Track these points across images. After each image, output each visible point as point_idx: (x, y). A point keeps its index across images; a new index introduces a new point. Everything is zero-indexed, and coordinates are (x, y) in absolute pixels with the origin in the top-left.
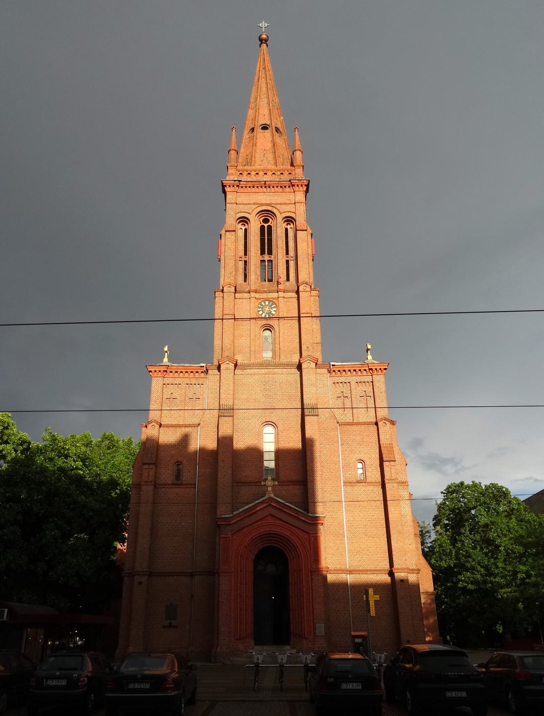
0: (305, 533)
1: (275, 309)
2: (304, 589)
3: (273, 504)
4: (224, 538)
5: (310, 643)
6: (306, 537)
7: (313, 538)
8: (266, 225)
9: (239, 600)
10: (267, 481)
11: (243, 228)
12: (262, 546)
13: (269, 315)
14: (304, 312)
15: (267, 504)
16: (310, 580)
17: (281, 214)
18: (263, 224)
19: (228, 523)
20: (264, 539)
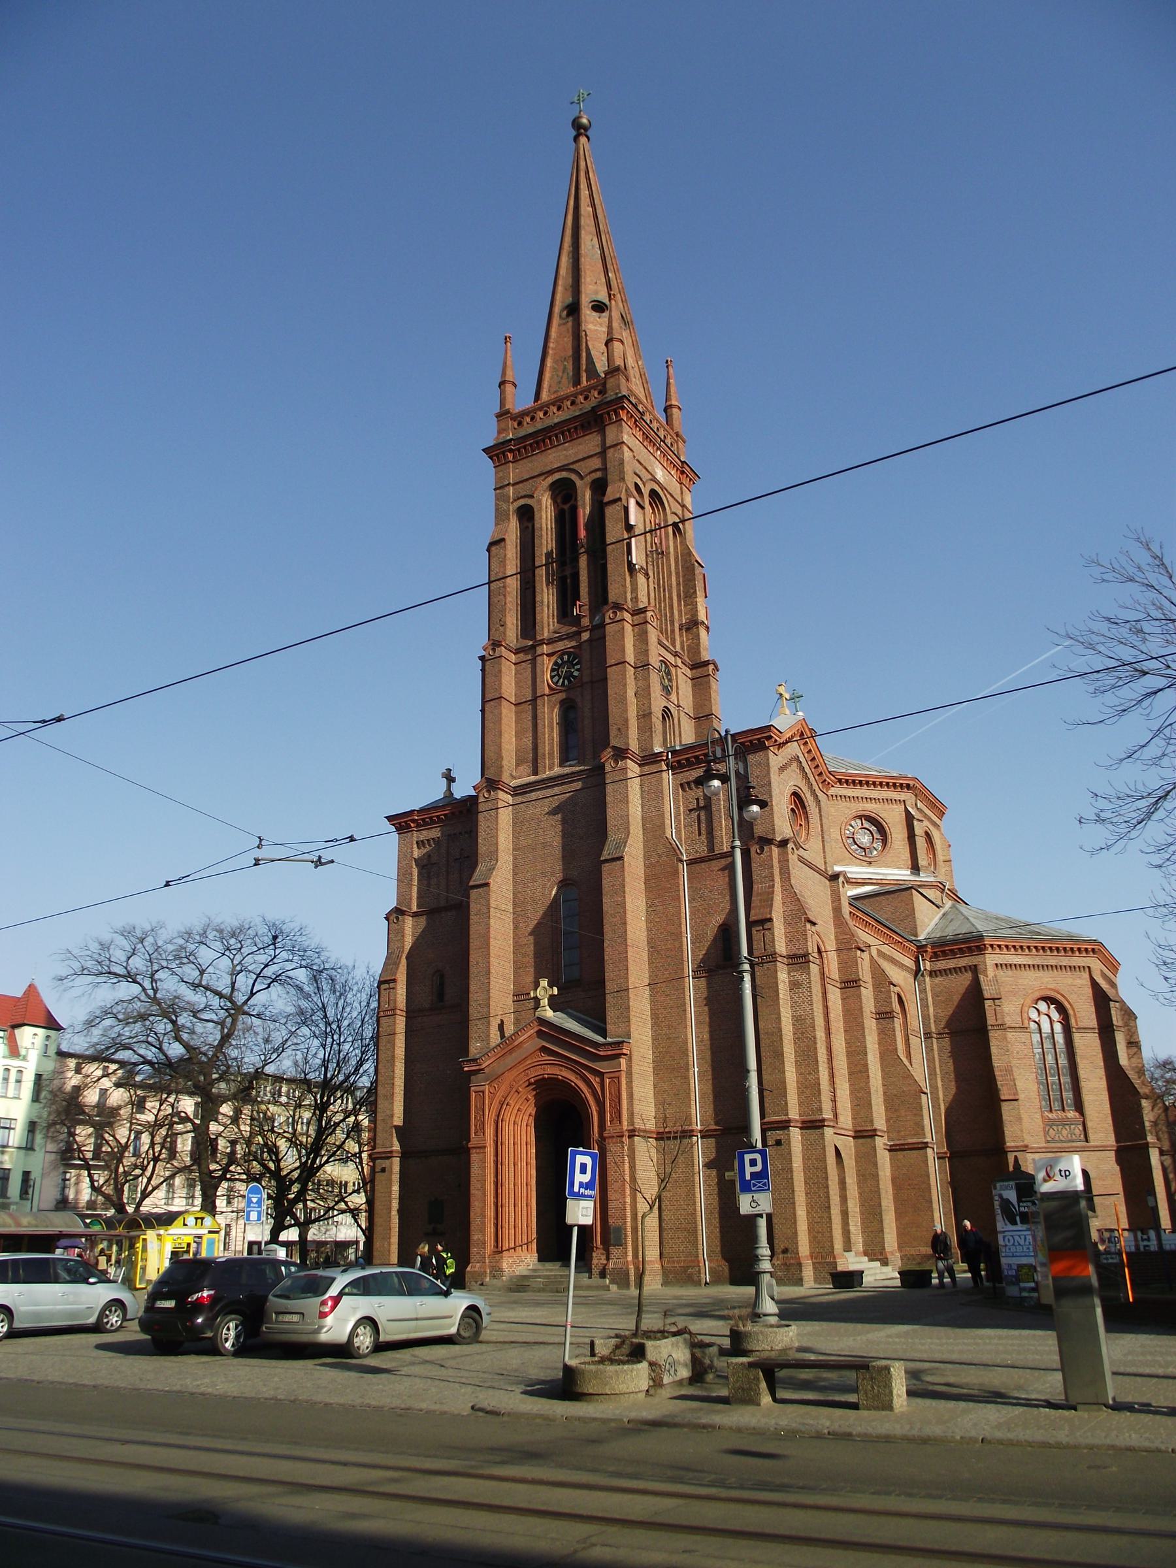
1: (578, 667)
8: (566, 507)
11: (530, 525)
13: (570, 681)
14: (613, 662)
17: (582, 478)
18: (562, 506)
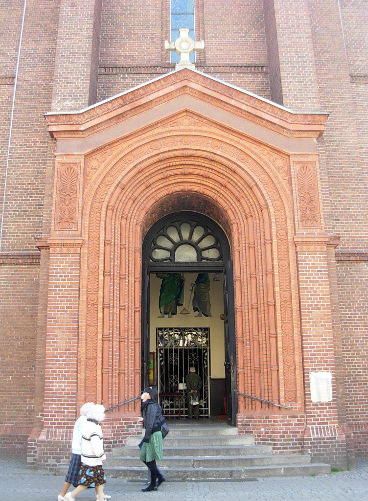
0: (275, 156)
2: (277, 289)
3: (193, 85)
4: (62, 164)
5: (294, 421)
6: (280, 163)
7: (298, 167)
9: (100, 315)
10: (178, 41)
12: (165, 192)
15: (179, 85)
16: (293, 265)
19: (74, 128)
20: (170, 173)
